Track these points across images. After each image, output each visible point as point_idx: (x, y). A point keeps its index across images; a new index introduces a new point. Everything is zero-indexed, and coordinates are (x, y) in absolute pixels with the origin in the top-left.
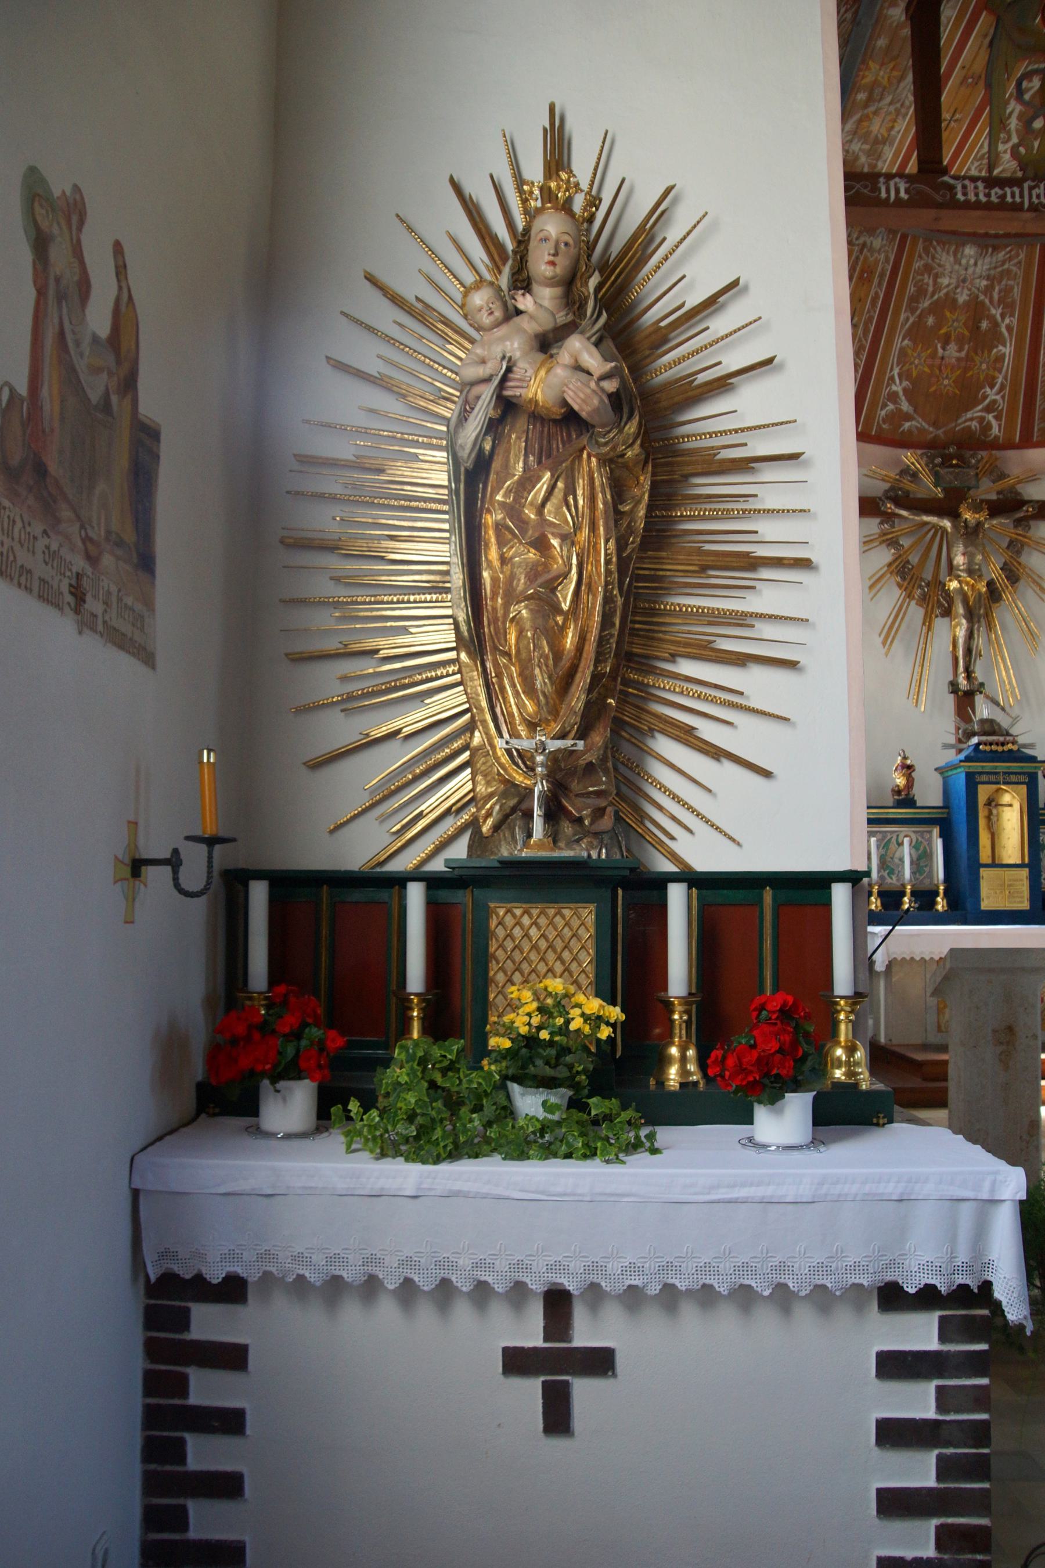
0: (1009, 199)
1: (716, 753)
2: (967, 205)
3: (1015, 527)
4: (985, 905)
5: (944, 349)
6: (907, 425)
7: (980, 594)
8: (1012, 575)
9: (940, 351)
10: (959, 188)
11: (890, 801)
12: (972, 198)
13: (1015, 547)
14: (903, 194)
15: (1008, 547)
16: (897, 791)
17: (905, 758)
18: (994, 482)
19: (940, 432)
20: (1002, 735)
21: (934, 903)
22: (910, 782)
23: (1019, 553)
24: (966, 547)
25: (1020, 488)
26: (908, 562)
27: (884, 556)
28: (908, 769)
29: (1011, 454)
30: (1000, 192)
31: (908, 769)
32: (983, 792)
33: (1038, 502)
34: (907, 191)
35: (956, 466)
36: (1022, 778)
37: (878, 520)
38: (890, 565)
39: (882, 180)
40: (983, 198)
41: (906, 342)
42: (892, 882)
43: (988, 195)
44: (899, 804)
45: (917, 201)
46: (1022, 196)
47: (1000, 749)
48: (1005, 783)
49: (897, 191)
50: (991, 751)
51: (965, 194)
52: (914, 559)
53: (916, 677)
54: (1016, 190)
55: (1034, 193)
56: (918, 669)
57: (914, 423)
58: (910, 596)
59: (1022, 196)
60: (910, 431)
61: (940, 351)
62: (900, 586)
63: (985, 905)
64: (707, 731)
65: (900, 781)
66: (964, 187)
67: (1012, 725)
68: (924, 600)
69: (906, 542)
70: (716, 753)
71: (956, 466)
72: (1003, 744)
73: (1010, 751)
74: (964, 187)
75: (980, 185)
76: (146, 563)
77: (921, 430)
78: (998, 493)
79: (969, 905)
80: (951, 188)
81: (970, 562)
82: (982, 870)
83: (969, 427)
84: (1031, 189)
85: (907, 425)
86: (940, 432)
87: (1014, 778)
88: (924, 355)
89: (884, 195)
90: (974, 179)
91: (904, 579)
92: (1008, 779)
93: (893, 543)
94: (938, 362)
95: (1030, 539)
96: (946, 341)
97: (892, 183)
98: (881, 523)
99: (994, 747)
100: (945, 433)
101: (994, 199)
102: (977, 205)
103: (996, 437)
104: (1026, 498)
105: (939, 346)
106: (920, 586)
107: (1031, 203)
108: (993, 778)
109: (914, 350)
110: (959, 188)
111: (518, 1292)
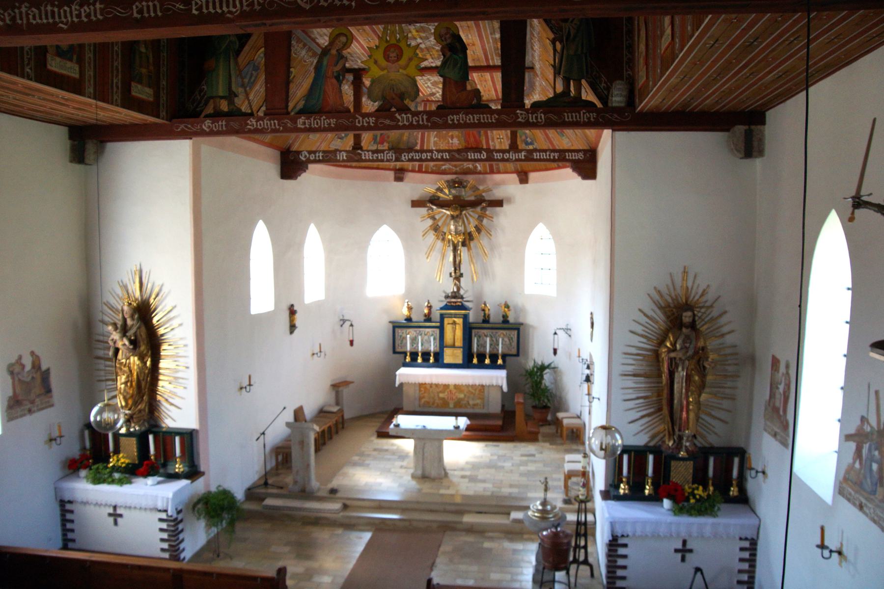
0: (380, 158)
1: (172, 404)
2: (366, 161)
3: (481, 210)
4: (446, 361)
5: (452, 140)
6: (443, 167)
7: (459, 242)
8: (478, 230)
9: (451, 141)
10: (363, 154)
11: (422, 318)
12: (367, 158)
13: (480, 218)
14: (345, 158)
15: (478, 219)
16: (425, 315)
17: (429, 303)
18: (474, 192)
19: (458, 169)
20: (459, 298)
21: (429, 359)
22: (430, 313)
23: (482, 221)
24: (454, 222)
25: (484, 194)
26: (438, 225)
27: (430, 222)
28: (430, 307)
29: (488, 176)
30: (376, 155)
31: (430, 307)
32: (446, 321)
33: (488, 201)
34: (346, 156)
35: (458, 187)
36: (461, 316)
37: (426, 209)
38: (431, 226)
39: (338, 153)
40: (371, 158)
41: (436, 139)
42: (425, 349)
43: (372, 157)
44: (426, 321)
45: (350, 159)
46: (384, 157)
47: (454, 304)
48: (455, 317)
49: (343, 156)
50: (451, 305)
51: (365, 156)
52: (440, 224)
53: (440, 269)
54: (382, 154)
55: (388, 155)
56: (440, 267)
57: (446, 166)
58: (438, 239)
59: (384, 157)
60: (445, 169)
61: (451, 141)
62: (434, 235)
63: (446, 361)
64: (171, 400)
65: (426, 311)
66: (365, 154)
67: (465, 293)
68: (443, 239)
69: (437, 217)
70: (172, 404)
71: (458, 187)
72: (455, 302)
73: (459, 305)
74: (365, 154)
75: (370, 153)
76: (48, 391)
77: (450, 169)
78: (475, 196)
79: (440, 360)
80: (361, 154)
81: (456, 229)
82: (445, 349)
83: (469, 167)
84: (387, 154)
85: (443, 167)
86: (458, 169)
87: (458, 316)
88: (444, 143)
89: (338, 158)
90: (368, 151)
91: (436, 232)
92: (456, 316)
93: (433, 218)
94: (450, 145)
95: (486, 215)
96: (452, 138)
97: (341, 154)
98: (428, 210)
99: (452, 304)
100: (460, 169)
101: (375, 158)
102: (369, 161)
103: (480, 170)
104: (487, 198)
105: (450, 140)
106: (442, 235)
107: (387, 159)
108: (450, 316)
109: (440, 141)
110: (363, 154)
111: (110, 505)
